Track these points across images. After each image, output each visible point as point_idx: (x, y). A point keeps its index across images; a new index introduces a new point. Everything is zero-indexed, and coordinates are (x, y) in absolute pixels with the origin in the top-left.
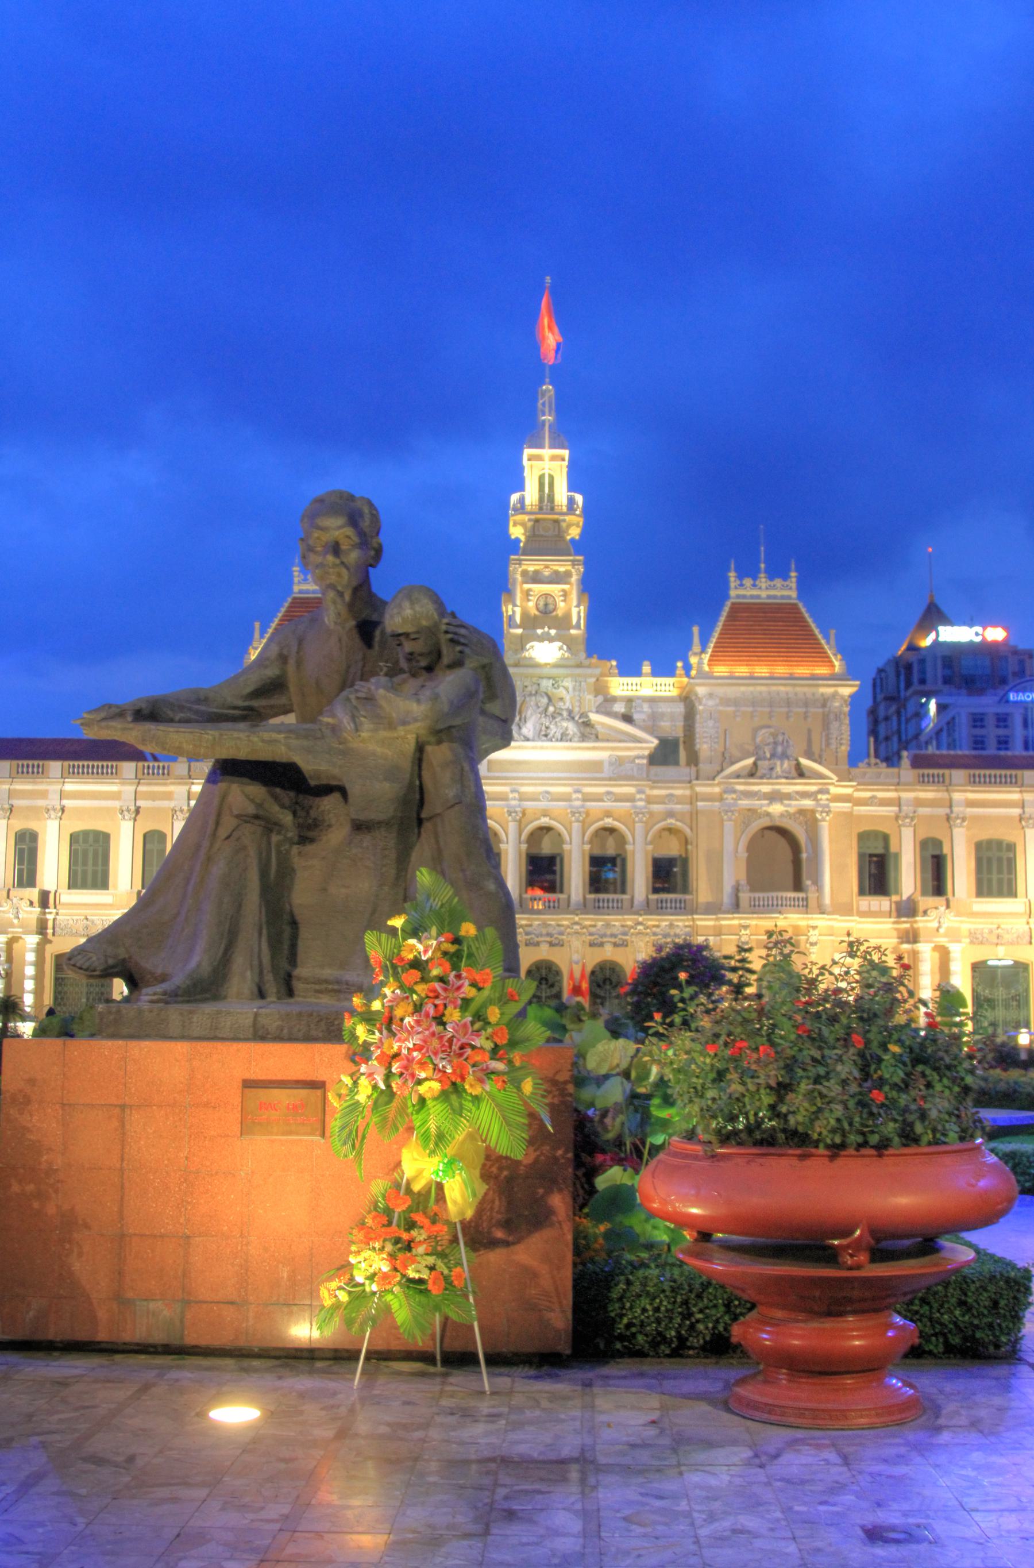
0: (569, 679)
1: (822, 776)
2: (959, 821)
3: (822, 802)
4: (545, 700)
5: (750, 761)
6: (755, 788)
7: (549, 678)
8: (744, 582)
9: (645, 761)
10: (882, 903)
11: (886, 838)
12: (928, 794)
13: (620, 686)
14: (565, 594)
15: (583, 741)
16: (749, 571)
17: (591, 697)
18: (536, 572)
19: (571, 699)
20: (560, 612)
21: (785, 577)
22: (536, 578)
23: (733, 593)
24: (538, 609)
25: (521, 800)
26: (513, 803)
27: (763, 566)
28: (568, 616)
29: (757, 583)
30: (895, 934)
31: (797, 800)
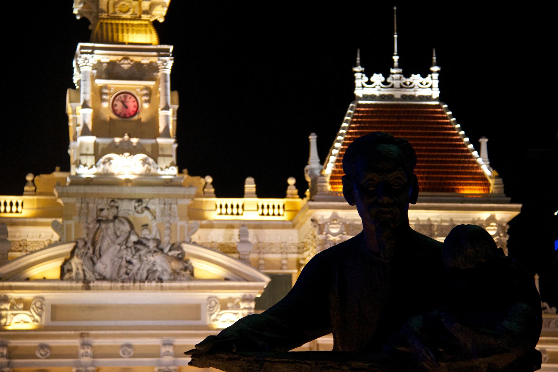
0: (157, 200)
4: (127, 227)
7: (131, 199)
8: (372, 79)
9: (253, 305)
13: (216, 208)
14: (150, 93)
15: (174, 280)
16: (378, 65)
18: (112, 64)
19: (158, 225)
20: (143, 116)
22: (111, 71)
23: (359, 92)
24: (114, 112)
25: (94, 356)
26: (85, 360)
27: (396, 58)
28: (154, 121)
29: (389, 80)
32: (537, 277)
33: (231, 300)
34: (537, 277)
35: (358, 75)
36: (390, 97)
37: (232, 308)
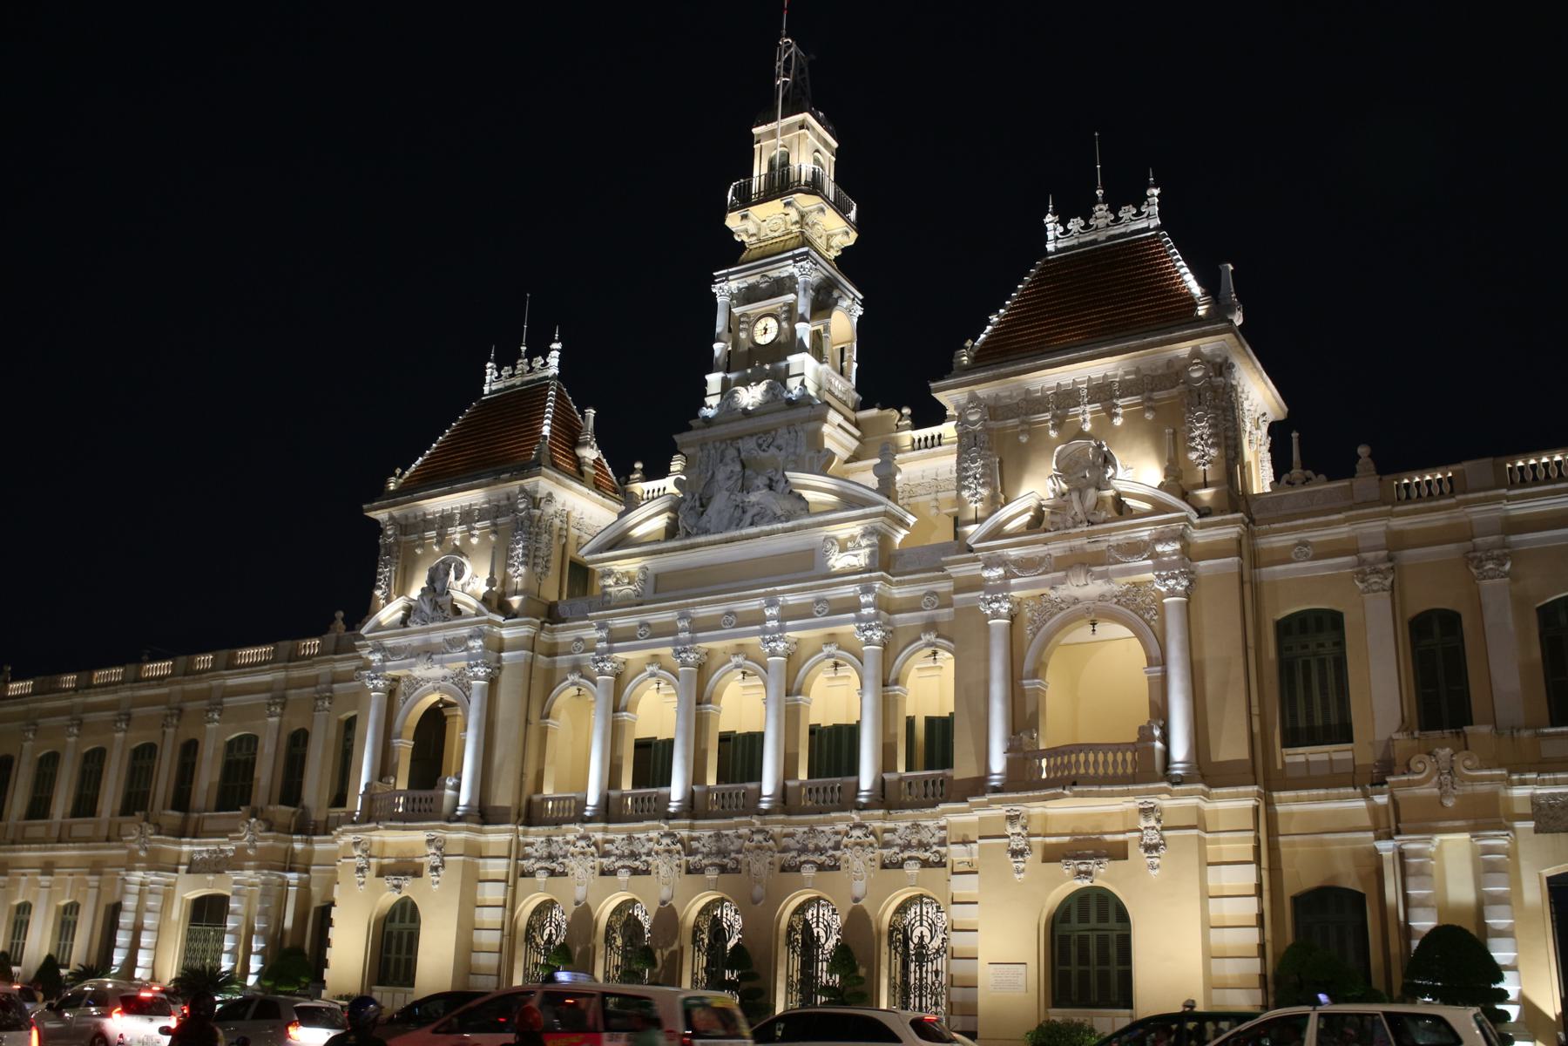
7: (751, 435)
8: (1069, 226)
16: (1074, 206)
18: (750, 288)
21: (1139, 200)
31: (1118, 562)
32: (1295, 435)
33: (852, 538)
34: (1295, 435)
35: (1050, 226)
36: (1094, 242)
37: (854, 549)
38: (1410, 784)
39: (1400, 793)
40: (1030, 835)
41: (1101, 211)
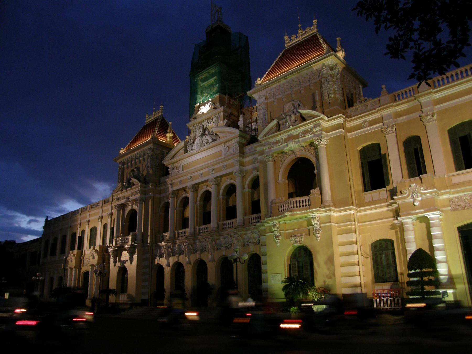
1: (314, 117)
2: (429, 117)
3: (317, 133)
5: (274, 123)
6: (279, 138)
10: (383, 193)
11: (378, 146)
12: (402, 107)
17: (222, 122)
21: (311, 24)
30: (391, 214)
31: (303, 137)
38: (402, 198)
39: (399, 202)
40: (280, 230)
41: (299, 31)
